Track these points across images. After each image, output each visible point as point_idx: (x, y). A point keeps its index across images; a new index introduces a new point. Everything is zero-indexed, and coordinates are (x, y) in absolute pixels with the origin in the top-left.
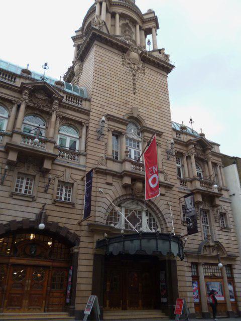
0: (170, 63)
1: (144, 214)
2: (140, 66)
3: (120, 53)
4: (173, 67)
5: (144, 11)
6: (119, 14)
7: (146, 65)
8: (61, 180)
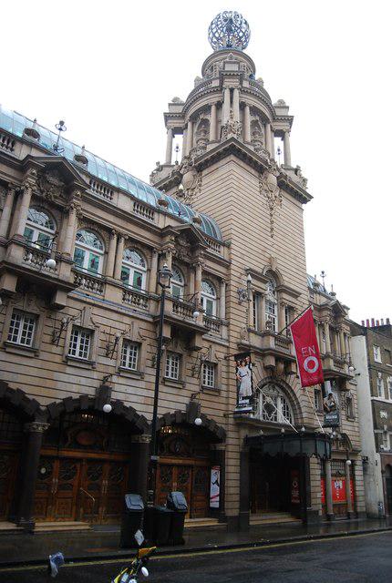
0: (307, 191)
1: (279, 400)
2: (277, 194)
3: (257, 174)
4: (311, 197)
5: (274, 101)
6: (250, 108)
8: (79, 324)
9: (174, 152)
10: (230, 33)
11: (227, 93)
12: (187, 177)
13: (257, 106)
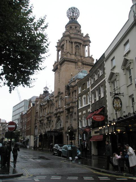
3: (74, 64)
7: (84, 66)
9: (59, 57)
10: (73, 15)
11: (66, 41)
12: (59, 67)
13: (76, 41)
